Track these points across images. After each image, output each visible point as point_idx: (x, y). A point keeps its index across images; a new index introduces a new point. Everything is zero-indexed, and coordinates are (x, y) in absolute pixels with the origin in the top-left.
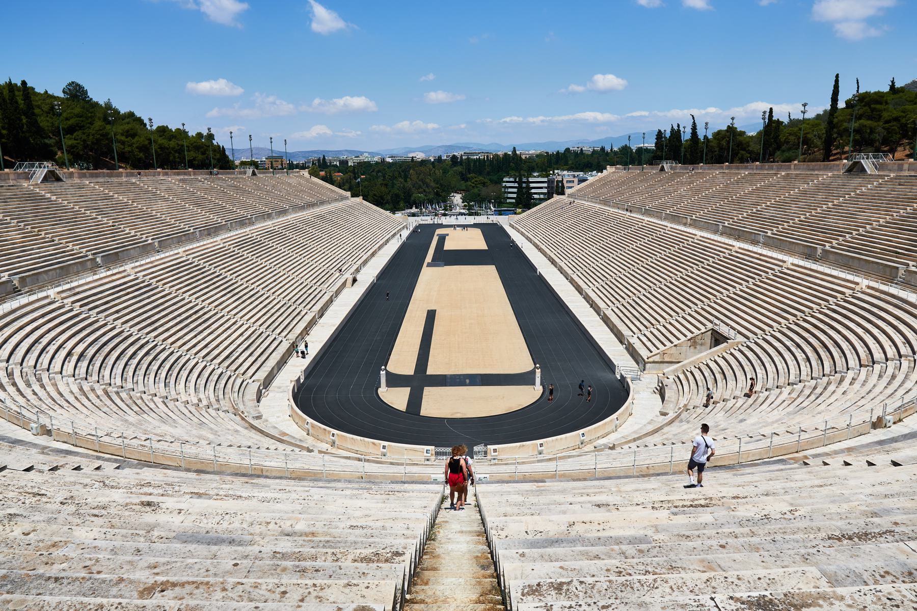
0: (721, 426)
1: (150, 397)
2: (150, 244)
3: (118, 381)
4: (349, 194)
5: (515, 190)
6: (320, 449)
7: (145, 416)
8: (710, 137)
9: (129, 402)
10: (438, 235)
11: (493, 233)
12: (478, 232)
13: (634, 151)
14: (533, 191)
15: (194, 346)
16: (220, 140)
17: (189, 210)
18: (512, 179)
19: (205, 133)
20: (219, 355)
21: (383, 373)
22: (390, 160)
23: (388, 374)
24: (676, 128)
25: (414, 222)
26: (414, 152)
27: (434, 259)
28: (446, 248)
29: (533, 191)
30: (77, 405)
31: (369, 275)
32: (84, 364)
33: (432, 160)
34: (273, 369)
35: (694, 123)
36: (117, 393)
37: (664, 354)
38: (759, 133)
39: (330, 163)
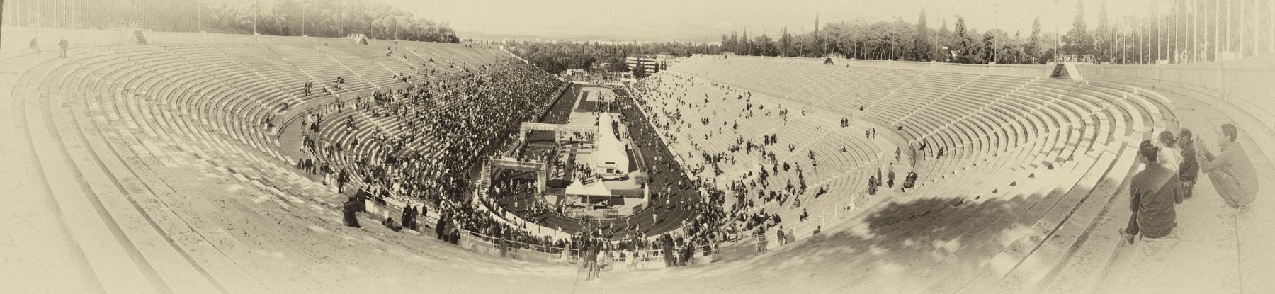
8: (754, 41)
12: (610, 91)
18: (634, 59)
24: (734, 34)
27: (579, 107)
28: (587, 100)
29: (645, 67)
38: (780, 40)
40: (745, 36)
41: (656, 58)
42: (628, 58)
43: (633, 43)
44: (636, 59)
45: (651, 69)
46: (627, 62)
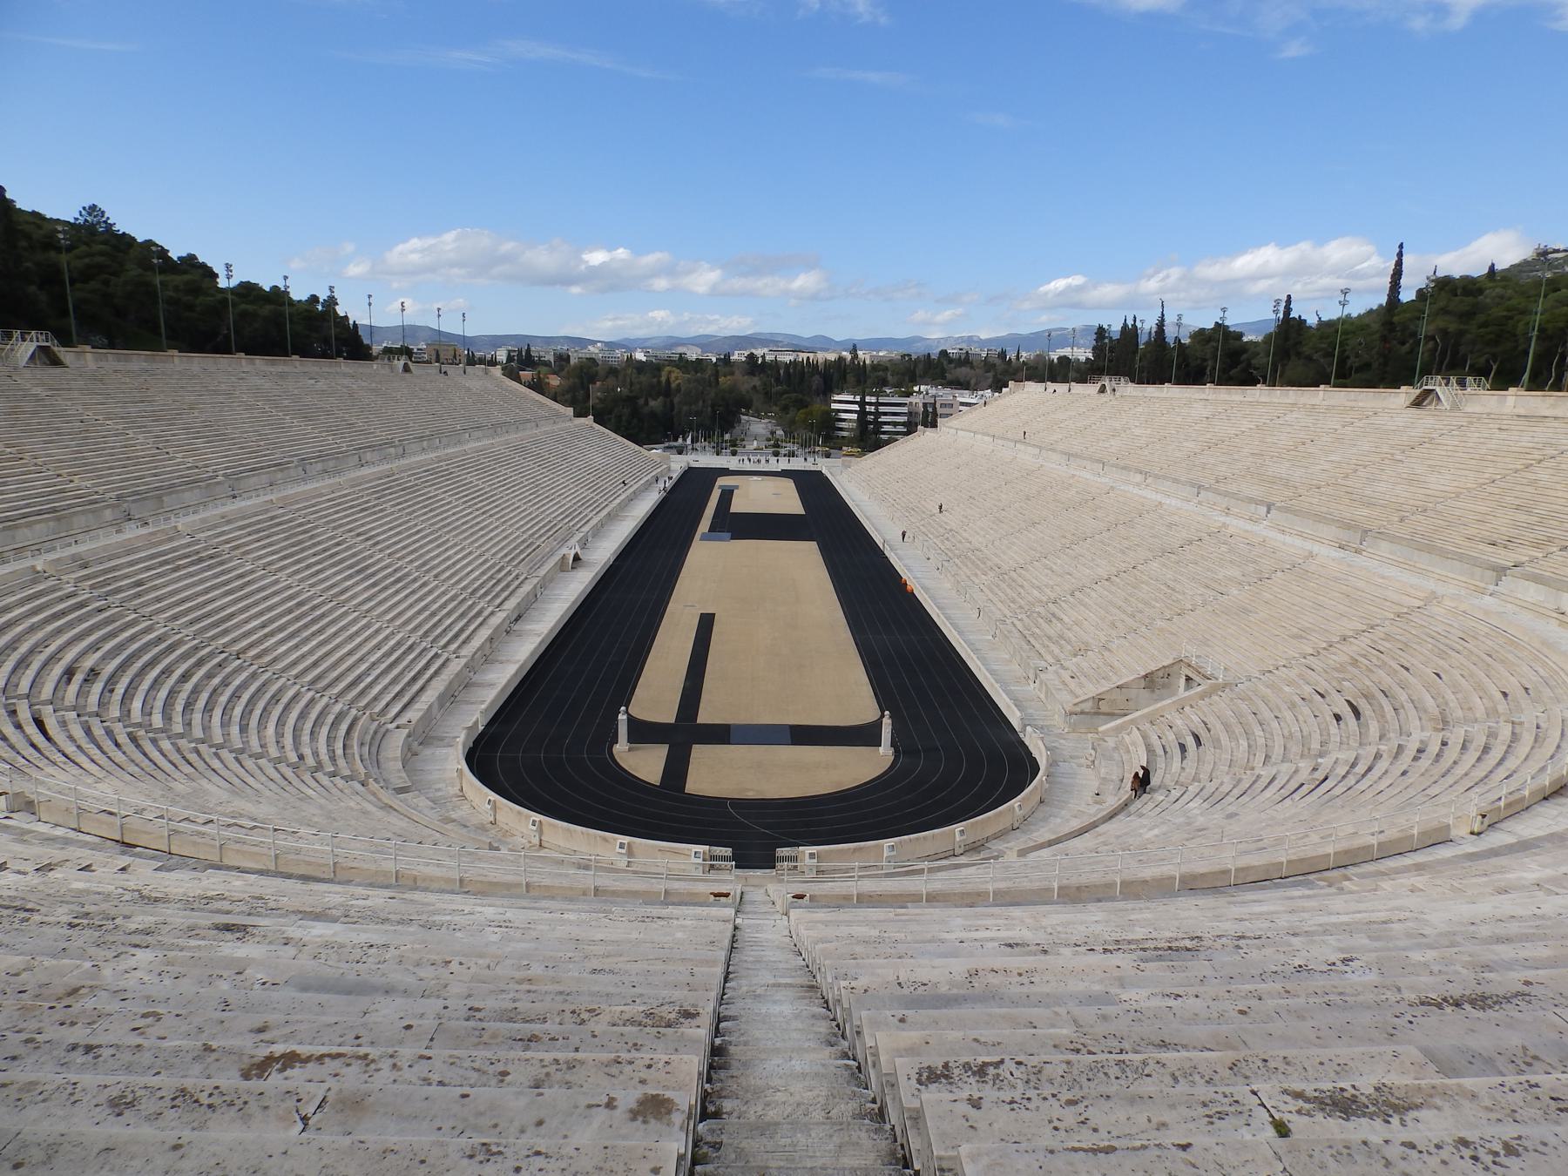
0: (1197, 824)
1: (214, 750)
2: (218, 483)
3: (157, 720)
4: (570, 411)
5: (855, 416)
6: (510, 846)
7: (204, 782)
8: (1186, 341)
9: (176, 757)
10: (720, 487)
11: (813, 487)
12: (789, 485)
13: (1055, 360)
14: (883, 419)
15: (294, 663)
16: (352, 309)
17: (291, 427)
18: (850, 398)
19: (323, 296)
20: (337, 679)
21: (622, 717)
22: (640, 356)
23: (632, 721)
24: (1130, 323)
25: (678, 464)
26: (683, 345)
28: (733, 510)
29: (883, 419)
30: (82, 759)
31: (604, 551)
32: (97, 687)
33: (714, 360)
34: (430, 706)
35: (1163, 315)
36: (154, 741)
37: (1100, 700)
38: (1268, 338)
39: (540, 357)
40: (1161, 325)
41: (909, 394)
42: (837, 397)
43: (847, 355)
44: (858, 399)
45: (895, 424)
46: (834, 406)
